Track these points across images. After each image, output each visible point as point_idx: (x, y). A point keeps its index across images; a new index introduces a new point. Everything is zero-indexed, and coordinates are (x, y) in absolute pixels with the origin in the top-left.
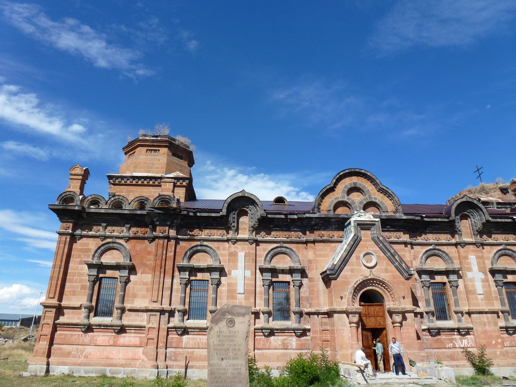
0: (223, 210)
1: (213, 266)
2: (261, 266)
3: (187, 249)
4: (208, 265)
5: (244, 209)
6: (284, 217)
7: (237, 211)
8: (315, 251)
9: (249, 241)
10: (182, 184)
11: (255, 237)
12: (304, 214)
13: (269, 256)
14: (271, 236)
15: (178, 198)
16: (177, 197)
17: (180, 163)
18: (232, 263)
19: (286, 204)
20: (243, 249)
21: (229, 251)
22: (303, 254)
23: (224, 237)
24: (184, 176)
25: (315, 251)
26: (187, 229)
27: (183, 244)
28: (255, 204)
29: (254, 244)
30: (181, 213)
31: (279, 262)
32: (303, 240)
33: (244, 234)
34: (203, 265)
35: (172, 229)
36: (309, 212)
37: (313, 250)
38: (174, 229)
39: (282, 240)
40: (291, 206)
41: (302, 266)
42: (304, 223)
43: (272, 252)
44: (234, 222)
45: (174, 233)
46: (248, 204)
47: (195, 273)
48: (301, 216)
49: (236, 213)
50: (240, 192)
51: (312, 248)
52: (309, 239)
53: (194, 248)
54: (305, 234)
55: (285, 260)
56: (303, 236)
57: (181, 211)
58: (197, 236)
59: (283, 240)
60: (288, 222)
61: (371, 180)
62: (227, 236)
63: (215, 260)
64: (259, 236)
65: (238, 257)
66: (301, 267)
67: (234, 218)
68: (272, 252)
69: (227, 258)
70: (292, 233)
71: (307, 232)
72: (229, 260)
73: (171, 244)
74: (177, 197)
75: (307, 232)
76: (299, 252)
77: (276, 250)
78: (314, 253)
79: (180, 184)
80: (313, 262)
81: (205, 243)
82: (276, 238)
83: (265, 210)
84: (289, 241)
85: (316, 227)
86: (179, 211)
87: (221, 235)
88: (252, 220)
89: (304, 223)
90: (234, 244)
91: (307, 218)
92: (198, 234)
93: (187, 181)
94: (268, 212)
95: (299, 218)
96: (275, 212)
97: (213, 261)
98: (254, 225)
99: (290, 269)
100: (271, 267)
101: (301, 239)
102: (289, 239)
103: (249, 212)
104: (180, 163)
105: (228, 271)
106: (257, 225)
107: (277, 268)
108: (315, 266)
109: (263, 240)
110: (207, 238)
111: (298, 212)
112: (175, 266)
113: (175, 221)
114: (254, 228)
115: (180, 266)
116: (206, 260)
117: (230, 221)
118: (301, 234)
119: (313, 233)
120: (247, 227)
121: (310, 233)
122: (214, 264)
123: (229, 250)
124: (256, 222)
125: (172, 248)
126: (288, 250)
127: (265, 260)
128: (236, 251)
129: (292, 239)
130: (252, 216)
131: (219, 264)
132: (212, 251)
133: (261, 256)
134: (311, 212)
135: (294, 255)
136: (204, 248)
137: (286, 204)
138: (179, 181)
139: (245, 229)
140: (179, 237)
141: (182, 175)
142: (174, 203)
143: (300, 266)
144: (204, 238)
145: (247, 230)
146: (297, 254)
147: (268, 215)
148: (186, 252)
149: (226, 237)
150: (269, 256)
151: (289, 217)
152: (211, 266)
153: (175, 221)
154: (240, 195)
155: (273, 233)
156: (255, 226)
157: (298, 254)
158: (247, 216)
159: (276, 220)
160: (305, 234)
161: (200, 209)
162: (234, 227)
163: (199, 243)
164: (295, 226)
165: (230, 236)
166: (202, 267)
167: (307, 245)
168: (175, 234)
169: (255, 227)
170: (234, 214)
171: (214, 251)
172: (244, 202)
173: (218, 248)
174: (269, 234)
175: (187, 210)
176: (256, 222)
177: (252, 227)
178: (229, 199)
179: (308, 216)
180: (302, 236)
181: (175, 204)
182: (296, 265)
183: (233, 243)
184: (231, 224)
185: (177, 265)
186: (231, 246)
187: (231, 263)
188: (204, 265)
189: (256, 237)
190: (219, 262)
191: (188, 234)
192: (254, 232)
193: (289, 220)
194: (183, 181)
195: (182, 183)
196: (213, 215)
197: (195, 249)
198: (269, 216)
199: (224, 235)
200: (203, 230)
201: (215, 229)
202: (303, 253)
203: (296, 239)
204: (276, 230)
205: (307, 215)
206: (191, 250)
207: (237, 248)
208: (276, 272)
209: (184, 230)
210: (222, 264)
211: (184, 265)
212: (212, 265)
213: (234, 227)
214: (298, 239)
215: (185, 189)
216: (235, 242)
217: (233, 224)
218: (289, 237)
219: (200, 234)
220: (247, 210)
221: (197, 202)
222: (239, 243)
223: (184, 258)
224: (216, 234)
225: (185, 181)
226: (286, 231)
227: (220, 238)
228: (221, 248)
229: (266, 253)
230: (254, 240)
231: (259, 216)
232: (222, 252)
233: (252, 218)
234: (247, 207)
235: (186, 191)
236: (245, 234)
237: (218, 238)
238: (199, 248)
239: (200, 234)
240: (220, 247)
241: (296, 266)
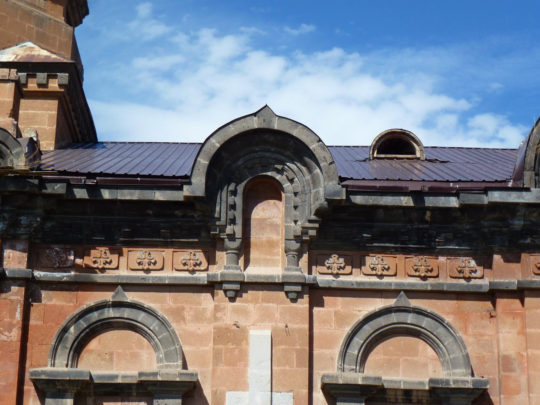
0: (193, 180)
1: (159, 378)
2: (328, 376)
3: (68, 318)
4: (141, 374)
5: (269, 174)
6: (412, 204)
7: (244, 184)
8: (524, 327)
9: (287, 288)
10: (45, 85)
11: (306, 274)
12: (485, 191)
13: (358, 340)
14: (366, 269)
15: (33, 135)
16: (27, 134)
17: (37, 12)
18: (226, 368)
19: (418, 155)
20: (266, 316)
21: (219, 324)
22: (482, 335)
23: (197, 275)
24: (54, 56)
25: (524, 327)
26: (68, 247)
27: (54, 302)
28: (307, 159)
29: (304, 303)
30: (44, 191)
31: (392, 365)
32: (481, 286)
33: (267, 263)
34: (123, 373)
35: (13, 248)
36: (503, 185)
37: (518, 321)
38: (20, 246)
39: (403, 284)
40: (438, 165)
41: (477, 378)
42: (486, 224)
43: (368, 329)
44: (233, 221)
45: (19, 263)
46: (283, 158)
47: (95, 401)
48: (472, 199)
49: (240, 189)
50: (255, 114)
51: (513, 314)
52: (502, 284)
53: (90, 315)
54: (487, 264)
55: (415, 359)
56: (480, 271)
57: (43, 183)
58: (103, 270)
59: (409, 284)
60: (427, 222)
62: (207, 270)
63: (168, 356)
64: (323, 269)
65: (247, 344)
66: (475, 382)
67: (233, 207)
68: (368, 329)
69: (209, 347)
70: (442, 259)
71: (497, 258)
72: (217, 356)
73: (12, 301)
74: (27, 134)
75: (497, 258)
76: (466, 332)
77: (382, 321)
78: (522, 332)
79: (40, 85)
80: (515, 365)
81: (131, 297)
82: (381, 276)
83: (342, 179)
84: (429, 288)
85: (529, 241)
86: (36, 182)
87: (186, 268)
88: (297, 213)
89: (486, 224)
90: (232, 299)
91: (495, 206)
92: (107, 266)
93: (64, 77)
94: (353, 186)
95: (464, 208)
96: (378, 184)
97: (159, 360)
98: (305, 230)
99: (432, 390)
100: (365, 383)
101: (473, 282)
102: (431, 281)
103: (286, 185)
104: (37, 12)
105: (214, 393)
106: (313, 233)
107: (386, 386)
108: (523, 379)
109: (334, 285)
110: (138, 277)
111: (463, 185)
112: (27, 376)
113: (24, 220)
114: (302, 242)
115: (43, 377)
116: (135, 356)
117: (219, 219)
118: (473, 263)
119: (518, 260)
120: (279, 237)
121: (507, 260)
122: (164, 371)
123: (216, 319)
124: (310, 221)
125: (12, 316)
126: (425, 322)
127: (344, 354)
128: (240, 324)
129: (440, 280)
130: (297, 199)
131: (180, 370)
132: (154, 325)
133: (329, 343)
134: (510, 184)
135: (448, 341)
136: (127, 313)
137: (418, 155)
138: (34, 76)
139: (271, 244)
140: (38, 274)
141: (44, 53)
142: (18, 155)
143: (469, 378)
144: (127, 277)
145: (281, 250)
146: (460, 334)
147: (352, 197)
148: (65, 330)
149: (204, 275)
150: (358, 340)
151: (430, 201)
152: (151, 378)
153: (24, 220)
154: (255, 124)
155: (371, 260)
156: (307, 233)
157: (464, 337)
158: (280, 199)
159: (381, 214)
160: (487, 264)
161: (113, 175)
162: (232, 237)
163: (108, 296)
164: (450, 236)
165: (219, 272)
166: (119, 381)
167: (494, 305)
168: (23, 266)
169: (305, 238)
170: (234, 193)
171: (163, 323)
172: (270, 151)
173: (178, 314)
174: (359, 264)
175: (67, 181)
176: (310, 221)
177: (297, 238)
178: (213, 140)
179: (498, 200)
180: (475, 272)
181: (23, 158)
182: (454, 374)
183: (231, 294)
184: (223, 229)
185: (32, 374)
186: (222, 305)
187: (222, 368)
188: (129, 373)
189: (310, 272)
190: (180, 362)
191: (69, 264)
192: (305, 257)
193: (428, 214)
194: (49, 77)
195: (44, 82)
196: (159, 196)
197: (95, 316)
198: (358, 199)
199: (197, 268)
200: (125, 250)
201: (166, 245)
202: (483, 331)
203: (454, 281)
204: (384, 251)
205: (496, 196)
206: (81, 321)
207: (245, 312)
208: (385, 400)
209: (57, 252)
210: (191, 369)
211: (58, 373)
212: (156, 374)
213: (232, 237)
214: (462, 281)
215: (54, 104)
216: (236, 291)
217: (229, 229)
218: (429, 274)
219: (114, 265)
220: (278, 177)
221: (102, 150)
222: (250, 295)
223: (55, 349)
224: (168, 265)
225: (55, 77)
226: (419, 252)
227: (185, 278)
228: (188, 314)
229: (348, 329)
230: (303, 285)
231: (322, 201)
232: (191, 327)
233: (296, 207)
234: (279, 167)
235: (62, 110)
236: (274, 263)
237: (175, 278)
238: (111, 313)
239: (114, 265)
240: (183, 309)
241: (457, 378)
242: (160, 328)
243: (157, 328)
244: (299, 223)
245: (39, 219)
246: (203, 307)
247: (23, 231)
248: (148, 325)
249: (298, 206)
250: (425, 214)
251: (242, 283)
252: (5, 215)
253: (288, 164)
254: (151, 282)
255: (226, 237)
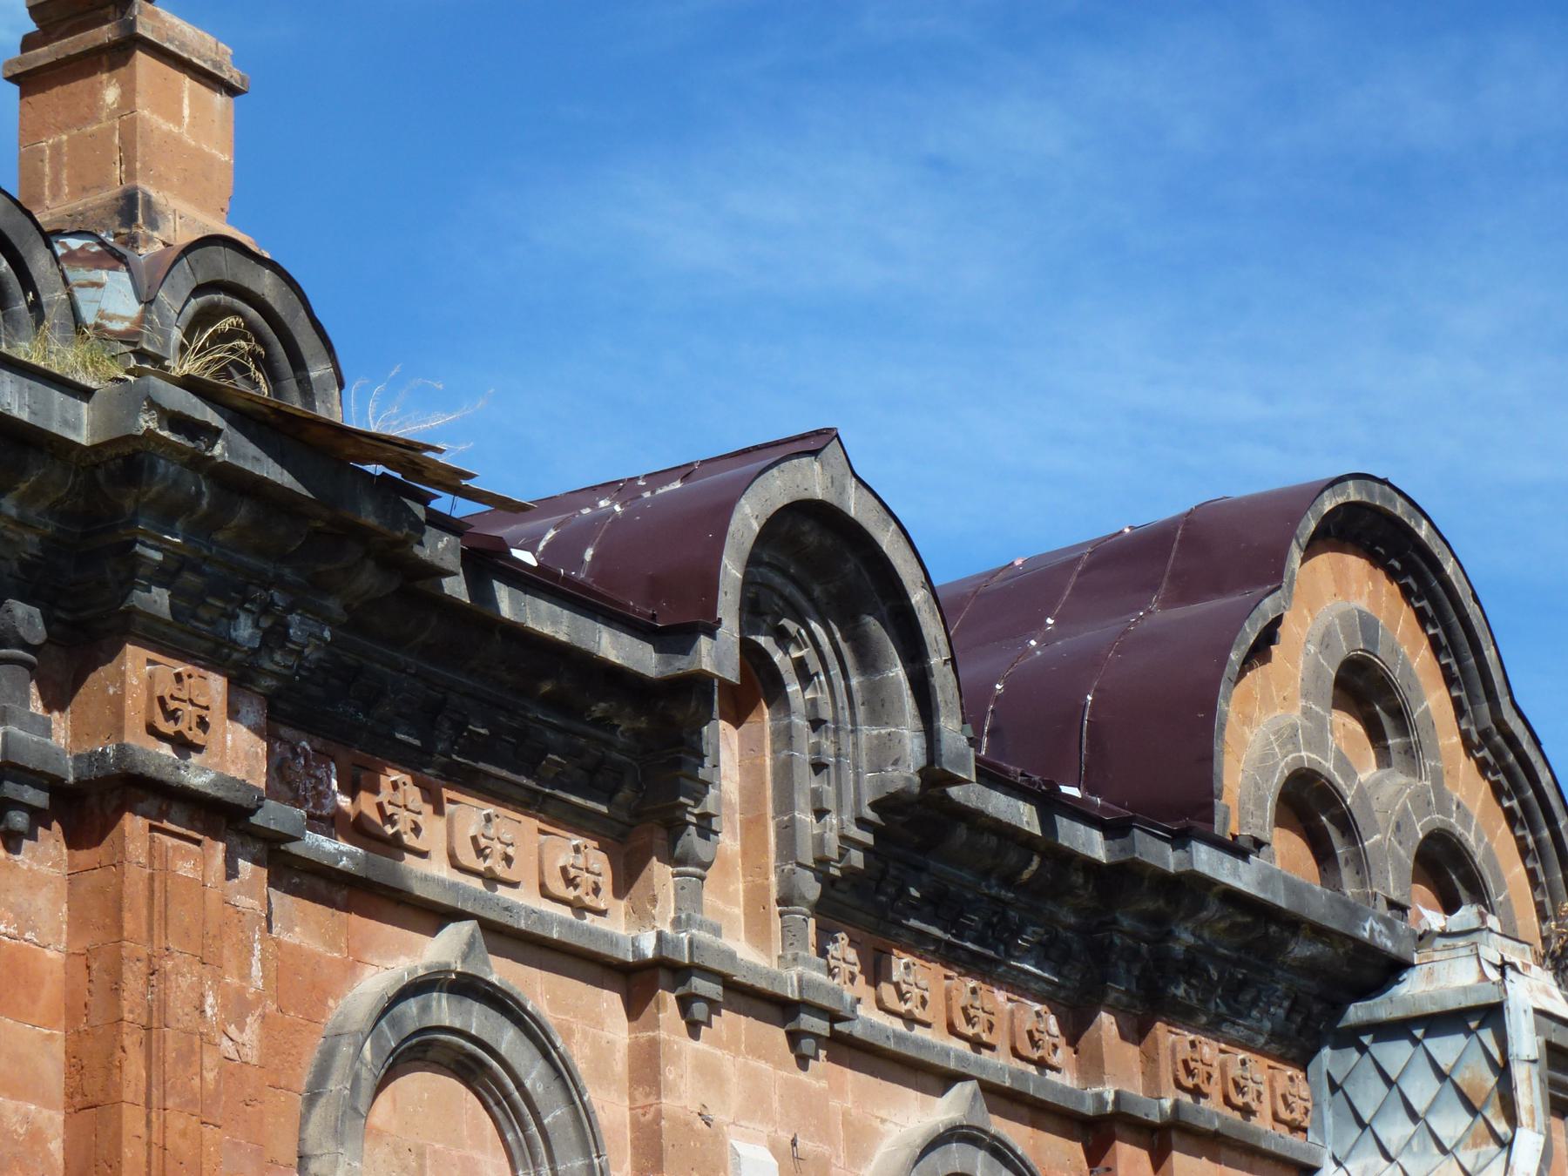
28: (873, 625)
46: (803, 602)
61: (1448, 630)
106: (857, 859)
172: (784, 572)
176: (861, 823)
234: (791, 626)
242: (547, 1088)
243: (540, 1089)
244: (832, 819)
245: (327, 634)
246: (611, 1036)
247: (277, 664)
248: (520, 1071)
249: (826, 766)
250: (1029, 862)
251: (729, 984)
252: (277, 596)
253: (814, 625)
254: (522, 925)
255: (694, 820)
